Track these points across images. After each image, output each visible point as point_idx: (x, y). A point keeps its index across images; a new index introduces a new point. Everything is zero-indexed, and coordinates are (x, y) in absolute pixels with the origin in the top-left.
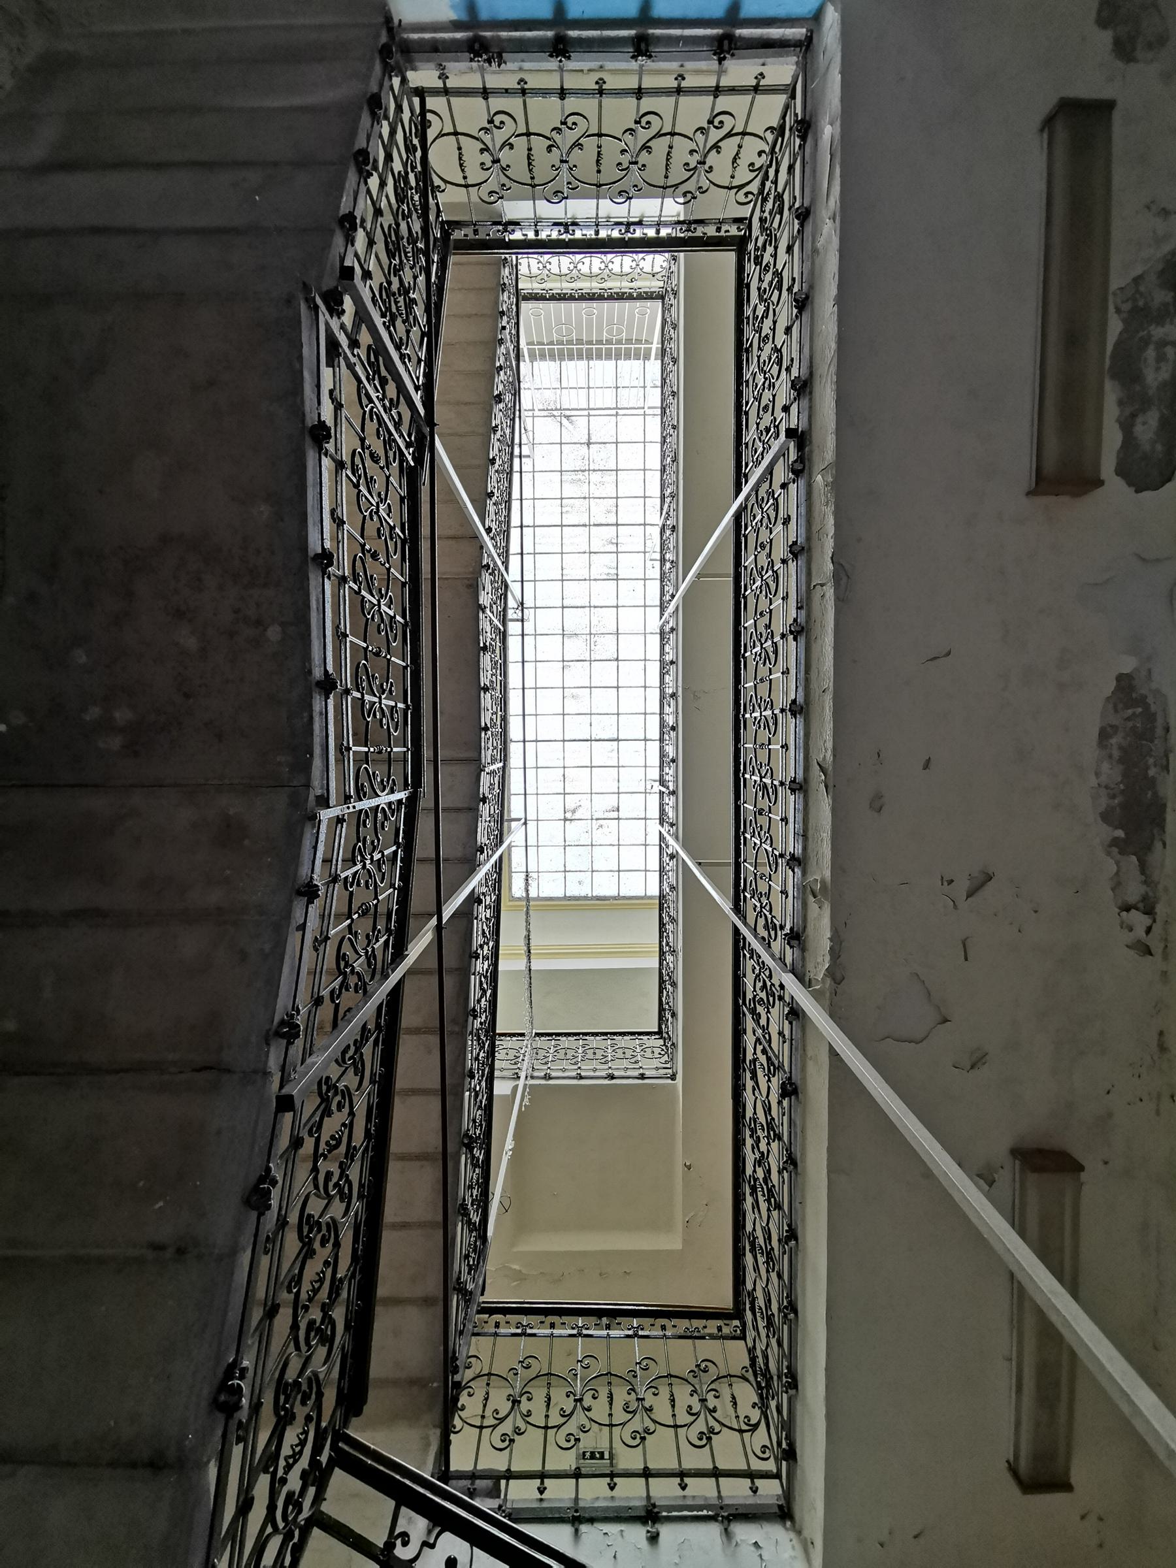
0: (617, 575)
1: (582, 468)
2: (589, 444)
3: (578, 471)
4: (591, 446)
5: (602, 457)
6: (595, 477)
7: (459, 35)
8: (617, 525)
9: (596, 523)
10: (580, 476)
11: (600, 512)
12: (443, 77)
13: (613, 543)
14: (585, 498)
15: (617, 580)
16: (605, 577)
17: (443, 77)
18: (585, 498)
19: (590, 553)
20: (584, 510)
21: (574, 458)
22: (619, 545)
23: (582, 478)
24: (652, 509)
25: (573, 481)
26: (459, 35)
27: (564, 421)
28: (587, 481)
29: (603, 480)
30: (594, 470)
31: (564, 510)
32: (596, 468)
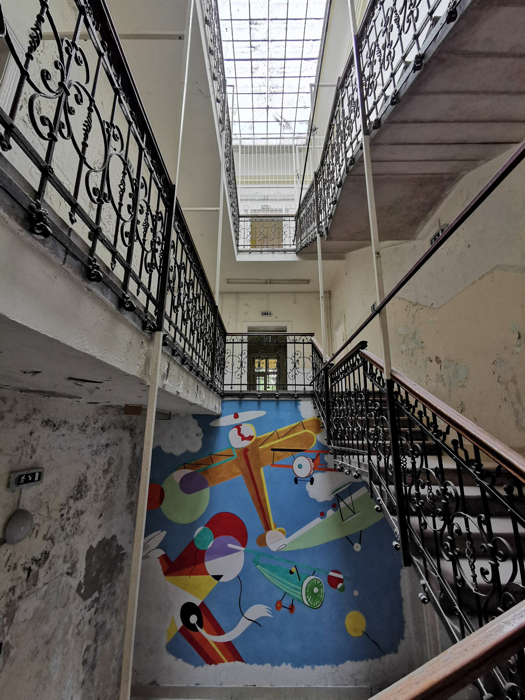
0: (250, 24)
1: (271, 95)
2: (268, 108)
3: (274, 93)
4: (266, 107)
5: (260, 101)
6: (264, 90)
7: (300, 399)
8: (251, 60)
9: (264, 61)
10: (273, 90)
11: (262, 68)
12: (305, 389)
13: (254, 47)
14: (271, 77)
15: (250, 19)
16: (258, 22)
17: (305, 389)
18: (271, 77)
19: (268, 41)
20: (271, 70)
21: (276, 101)
22: (249, 46)
23: (271, 89)
24: (231, 70)
25: (277, 87)
26: (300, 399)
27: (280, 119)
28: (269, 87)
29: (260, 88)
30: (265, 93)
31: (283, 70)
32: (264, 95)
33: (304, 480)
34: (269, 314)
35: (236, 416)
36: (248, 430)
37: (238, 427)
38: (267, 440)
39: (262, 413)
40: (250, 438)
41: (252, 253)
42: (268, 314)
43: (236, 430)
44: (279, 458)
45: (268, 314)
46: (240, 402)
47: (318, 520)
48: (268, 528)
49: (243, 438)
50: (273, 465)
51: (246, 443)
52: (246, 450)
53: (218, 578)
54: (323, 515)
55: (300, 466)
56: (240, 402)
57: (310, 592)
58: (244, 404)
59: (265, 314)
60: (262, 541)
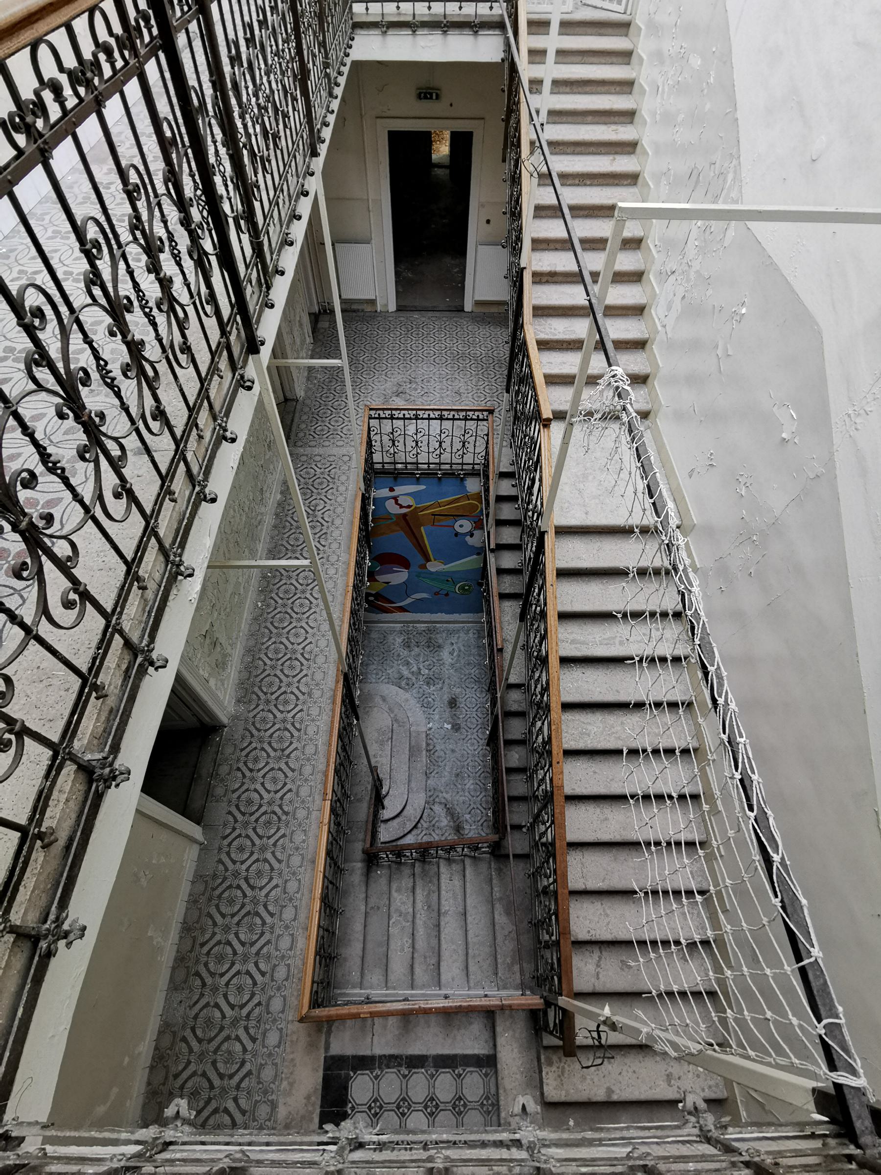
33: (465, 534)
34: (434, 97)
35: (392, 490)
36: (405, 501)
37: (395, 499)
38: (427, 508)
39: (423, 487)
40: (409, 507)
41: (390, 32)
42: (431, 98)
43: (393, 501)
44: (439, 521)
45: (431, 98)
46: (395, 479)
47: (475, 556)
48: (428, 560)
49: (401, 507)
50: (433, 525)
51: (404, 511)
52: (404, 515)
53: (388, 583)
54: (478, 554)
55: (461, 526)
56: (395, 479)
57: (462, 588)
58: (399, 480)
59: (426, 98)
60: (424, 567)
